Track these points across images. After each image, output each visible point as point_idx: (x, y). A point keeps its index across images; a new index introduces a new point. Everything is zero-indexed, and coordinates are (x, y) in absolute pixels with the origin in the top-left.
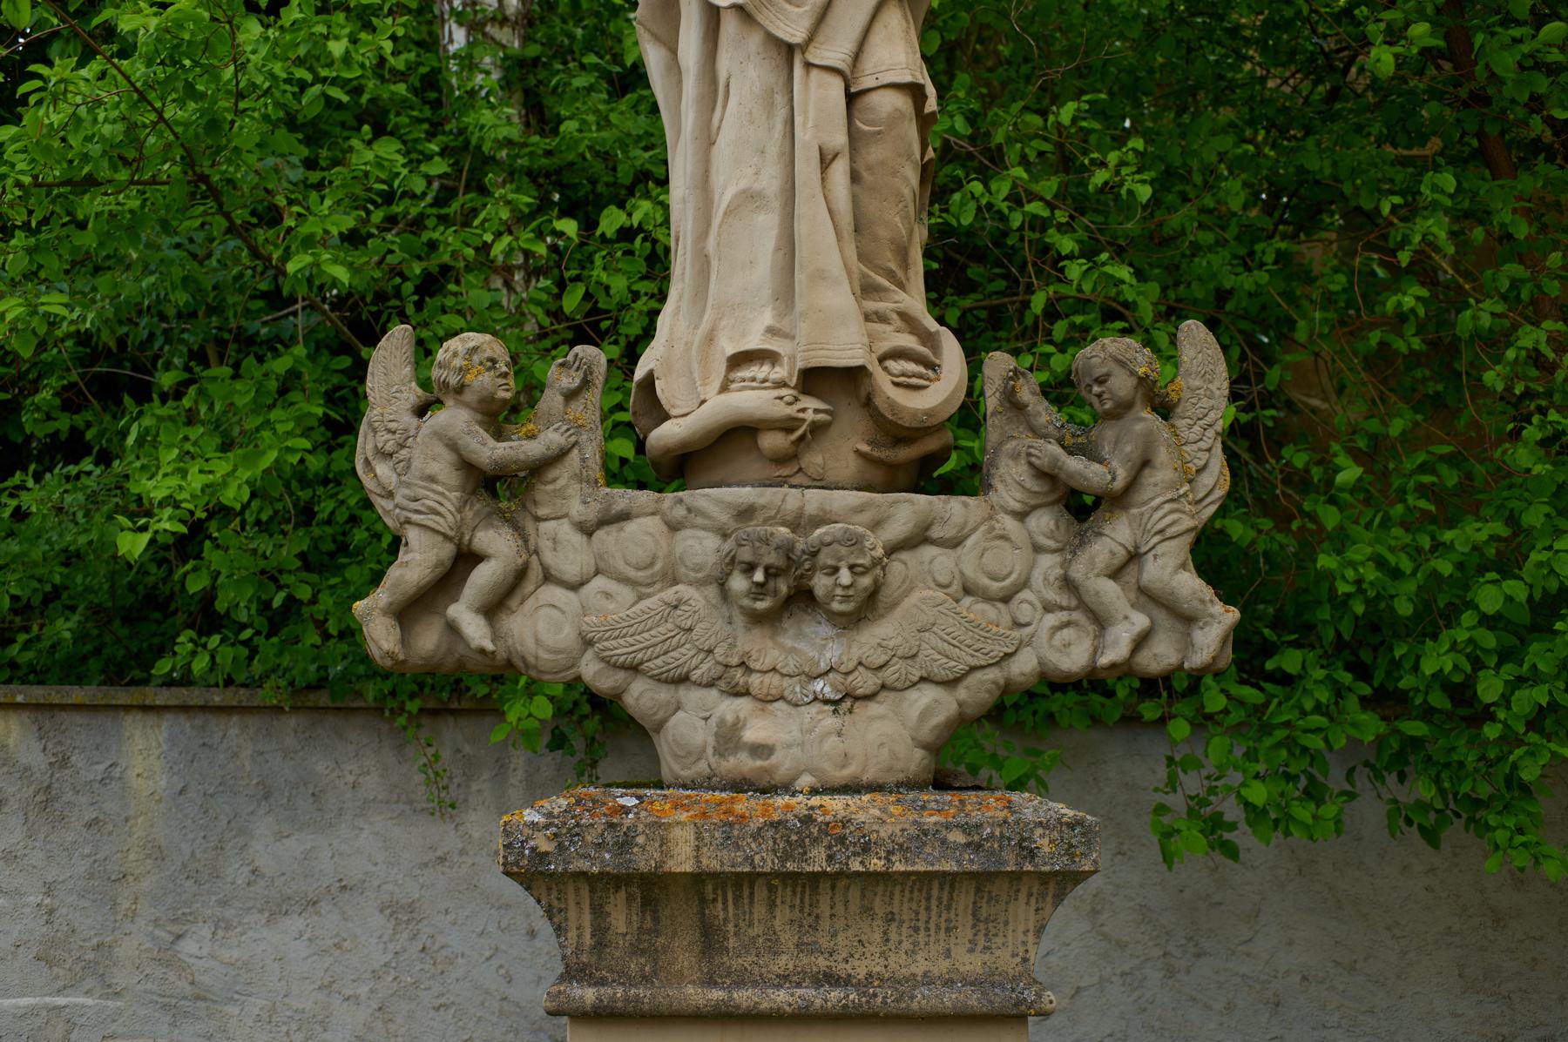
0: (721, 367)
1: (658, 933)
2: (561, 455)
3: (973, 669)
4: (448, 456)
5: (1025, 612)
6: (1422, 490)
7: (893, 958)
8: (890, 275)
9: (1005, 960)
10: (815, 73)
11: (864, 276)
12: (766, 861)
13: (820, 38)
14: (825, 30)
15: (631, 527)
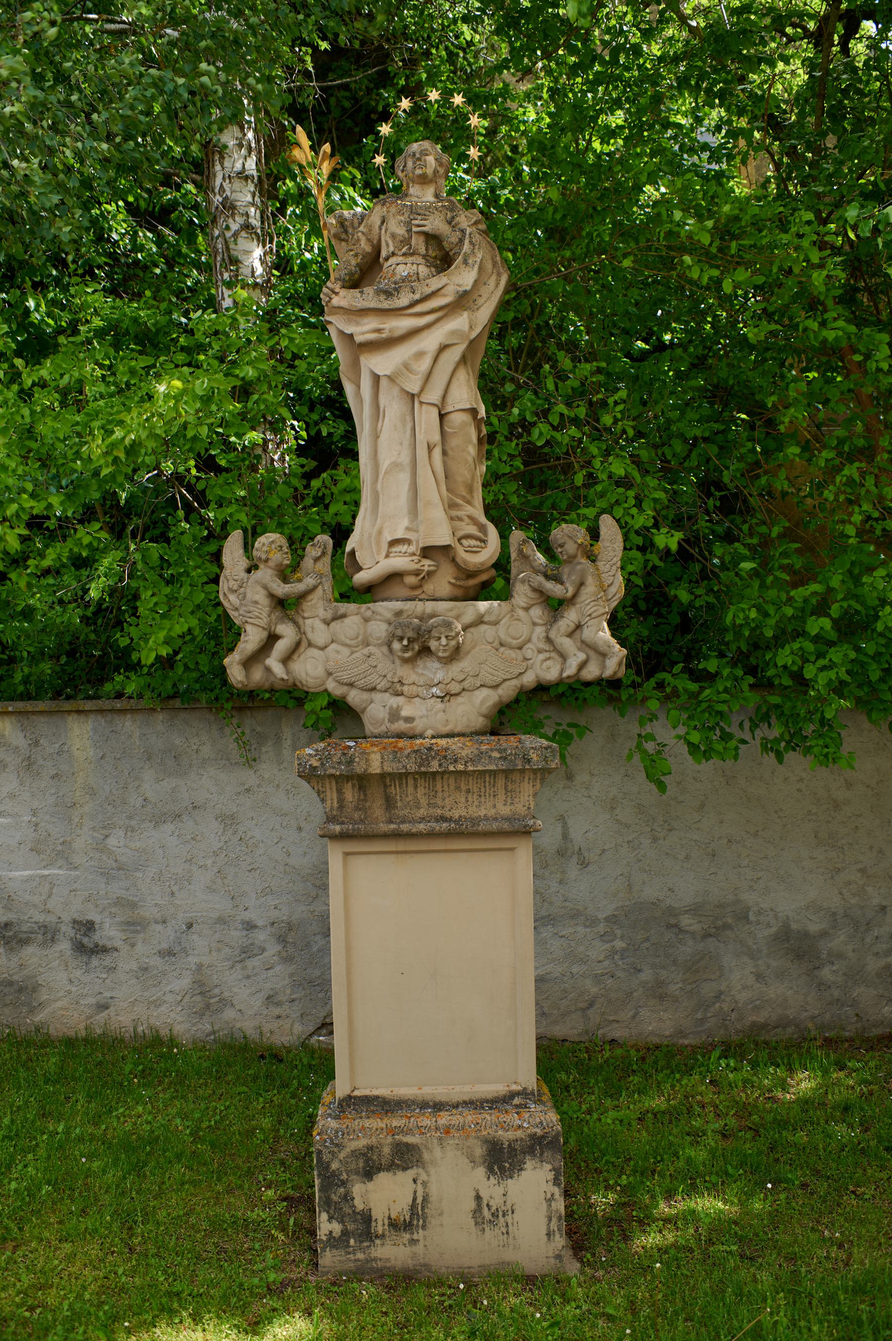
0: (385, 546)
1: (366, 801)
2: (315, 588)
3: (505, 680)
4: (264, 592)
5: (529, 654)
6: (783, 568)
7: (470, 809)
8: (463, 498)
9: (520, 809)
10: (424, 406)
11: (451, 499)
12: (412, 767)
13: (426, 389)
14: (429, 385)
15: (347, 621)
